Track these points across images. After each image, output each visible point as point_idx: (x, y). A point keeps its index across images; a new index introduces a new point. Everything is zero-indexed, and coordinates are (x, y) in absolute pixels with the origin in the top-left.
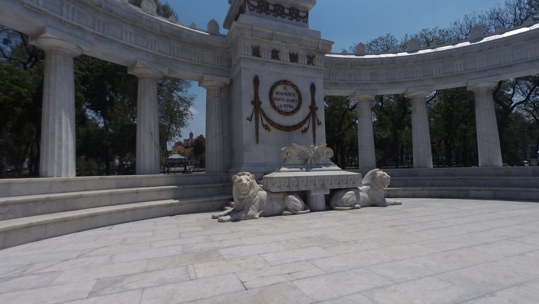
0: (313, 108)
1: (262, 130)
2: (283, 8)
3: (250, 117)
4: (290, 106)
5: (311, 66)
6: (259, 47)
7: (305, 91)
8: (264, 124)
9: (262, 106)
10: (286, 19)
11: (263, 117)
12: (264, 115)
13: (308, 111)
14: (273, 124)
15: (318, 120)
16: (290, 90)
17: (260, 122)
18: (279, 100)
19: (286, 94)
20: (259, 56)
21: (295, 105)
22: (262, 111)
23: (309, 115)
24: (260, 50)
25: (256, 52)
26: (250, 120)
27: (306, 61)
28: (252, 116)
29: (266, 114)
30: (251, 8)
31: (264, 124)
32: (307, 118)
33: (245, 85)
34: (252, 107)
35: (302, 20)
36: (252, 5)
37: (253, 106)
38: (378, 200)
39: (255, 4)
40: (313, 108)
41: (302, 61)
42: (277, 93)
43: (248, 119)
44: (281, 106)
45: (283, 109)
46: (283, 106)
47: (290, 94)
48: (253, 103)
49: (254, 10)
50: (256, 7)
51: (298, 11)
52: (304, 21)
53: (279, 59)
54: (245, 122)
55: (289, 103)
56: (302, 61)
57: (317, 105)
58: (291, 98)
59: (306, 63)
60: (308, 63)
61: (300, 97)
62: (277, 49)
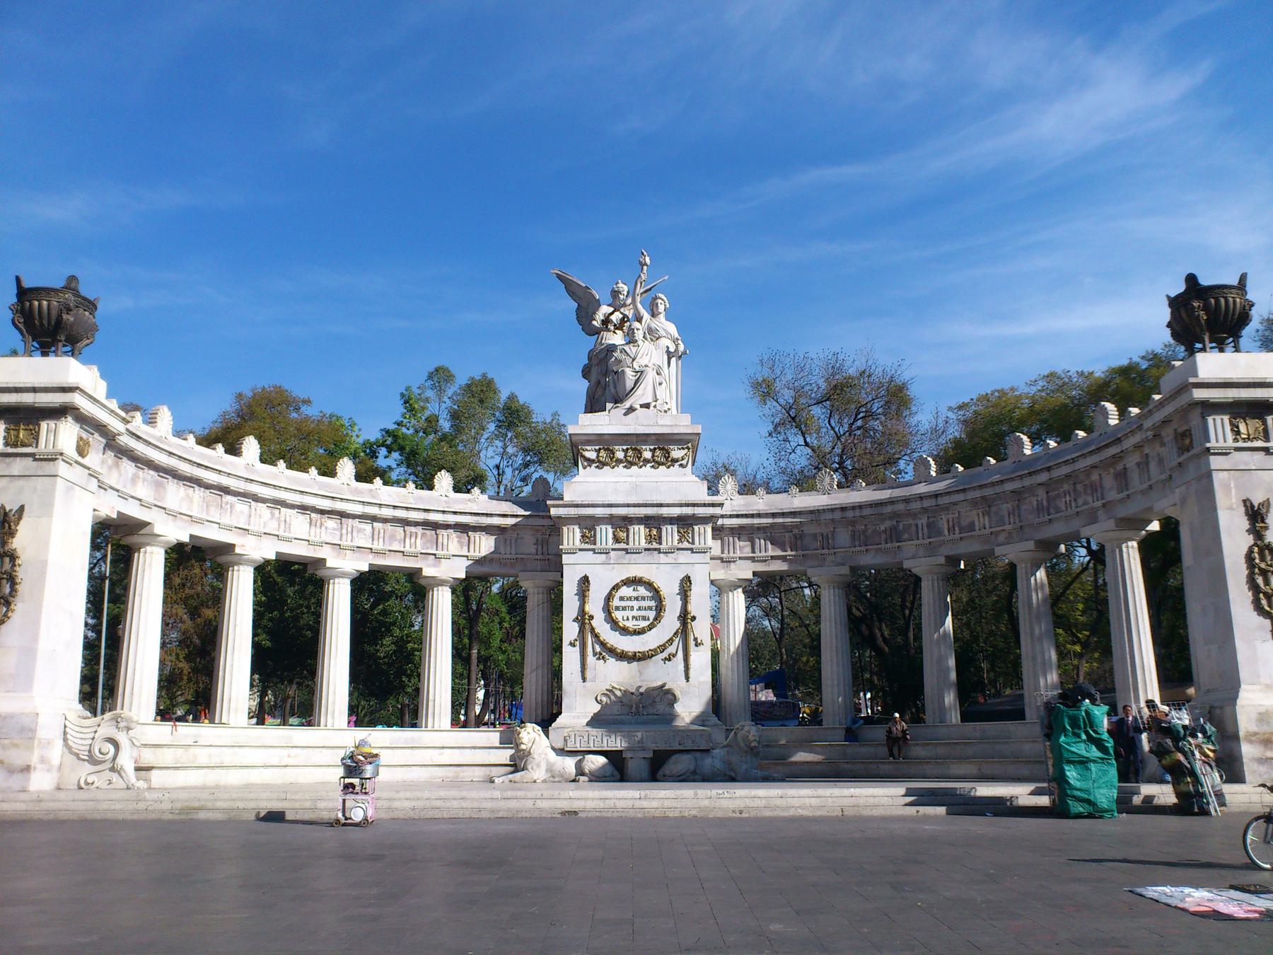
0: (685, 618)
1: (591, 659)
13: (677, 625)
14: (612, 651)
15: (696, 639)
18: (624, 609)
19: (637, 598)
21: (652, 614)
26: (572, 644)
27: (676, 537)
34: (576, 625)
40: (685, 618)
42: (622, 599)
45: (630, 624)
47: (643, 598)
48: (576, 620)
50: (593, 461)
52: (681, 465)
54: (566, 649)
55: (643, 613)
59: (676, 542)
60: (680, 541)
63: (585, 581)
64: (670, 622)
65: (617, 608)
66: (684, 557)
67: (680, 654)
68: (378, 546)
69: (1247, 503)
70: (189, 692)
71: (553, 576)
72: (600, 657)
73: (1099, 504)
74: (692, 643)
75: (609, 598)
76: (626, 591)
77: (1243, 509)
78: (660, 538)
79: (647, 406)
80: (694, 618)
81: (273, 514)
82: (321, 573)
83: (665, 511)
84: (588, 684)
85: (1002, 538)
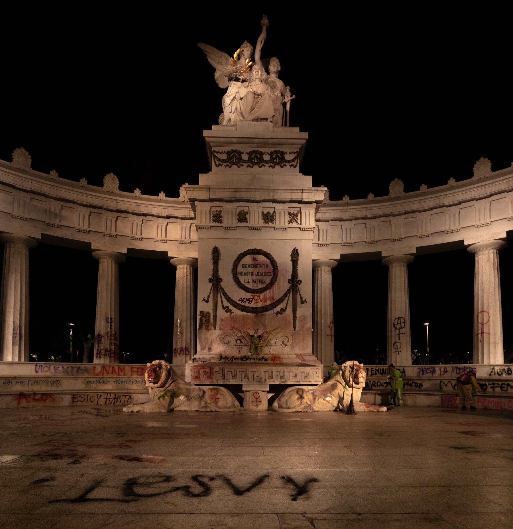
2: (261, 154)
3: (206, 299)
5: (295, 224)
6: (220, 212)
8: (225, 306)
9: (222, 284)
11: (223, 297)
12: (225, 294)
13: (288, 286)
18: (246, 274)
19: (255, 266)
20: (221, 222)
21: (268, 279)
22: (222, 289)
23: (289, 291)
24: (222, 215)
25: (217, 218)
26: (207, 301)
27: (287, 219)
28: (209, 297)
29: (228, 294)
30: (218, 163)
31: (225, 306)
32: (285, 295)
35: (288, 165)
36: (219, 160)
37: (211, 284)
39: (224, 157)
42: (244, 266)
43: (204, 300)
44: (249, 282)
45: (249, 286)
46: (251, 281)
47: (261, 266)
48: (210, 280)
49: (222, 165)
50: (223, 161)
51: (283, 154)
52: (292, 165)
53: (247, 222)
55: (260, 278)
57: (300, 278)
58: (263, 270)
59: (287, 223)
60: (290, 222)
62: (246, 210)
64: (282, 285)
65: (241, 274)
72: (227, 310)
74: (299, 300)
76: (248, 260)
78: (275, 219)
80: (300, 281)
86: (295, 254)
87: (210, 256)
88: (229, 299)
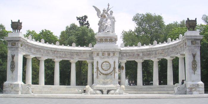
0: (114, 68)
4: (107, 68)
7: (112, 63)
10: (108, 43)
14: (102, 73)
16: (107, 63)
17: (98, 73)
18: (104, 66)
21: (109, 68)
27: (113, 55)
33: (95, 64)
38: (121, 93)
39: (99, 40)
40: (114, 68)
41: (112, 54)
45: (105, 69)
54: (94, 73)
56: (112, 54)
61: (110, 65)
63: (97, 62)
64: (112, 69)
66: (114, 58)
67: (113, 74)
68: (63, 56)
69: (193, 54)
70: (35, 81)
71: (92, 61)
72: (100, 74)
73: (178, 51)
75: (102, 65)
76: (104, 64)
77: (192, 55)
79: (108, 32)
81: (47, 52)
82: (54, 61)
83: (111, 50)
84: (98, 79)
85: (165, 55)
86: (114, 62)
87: (96, 63)
88: (100, 72)
